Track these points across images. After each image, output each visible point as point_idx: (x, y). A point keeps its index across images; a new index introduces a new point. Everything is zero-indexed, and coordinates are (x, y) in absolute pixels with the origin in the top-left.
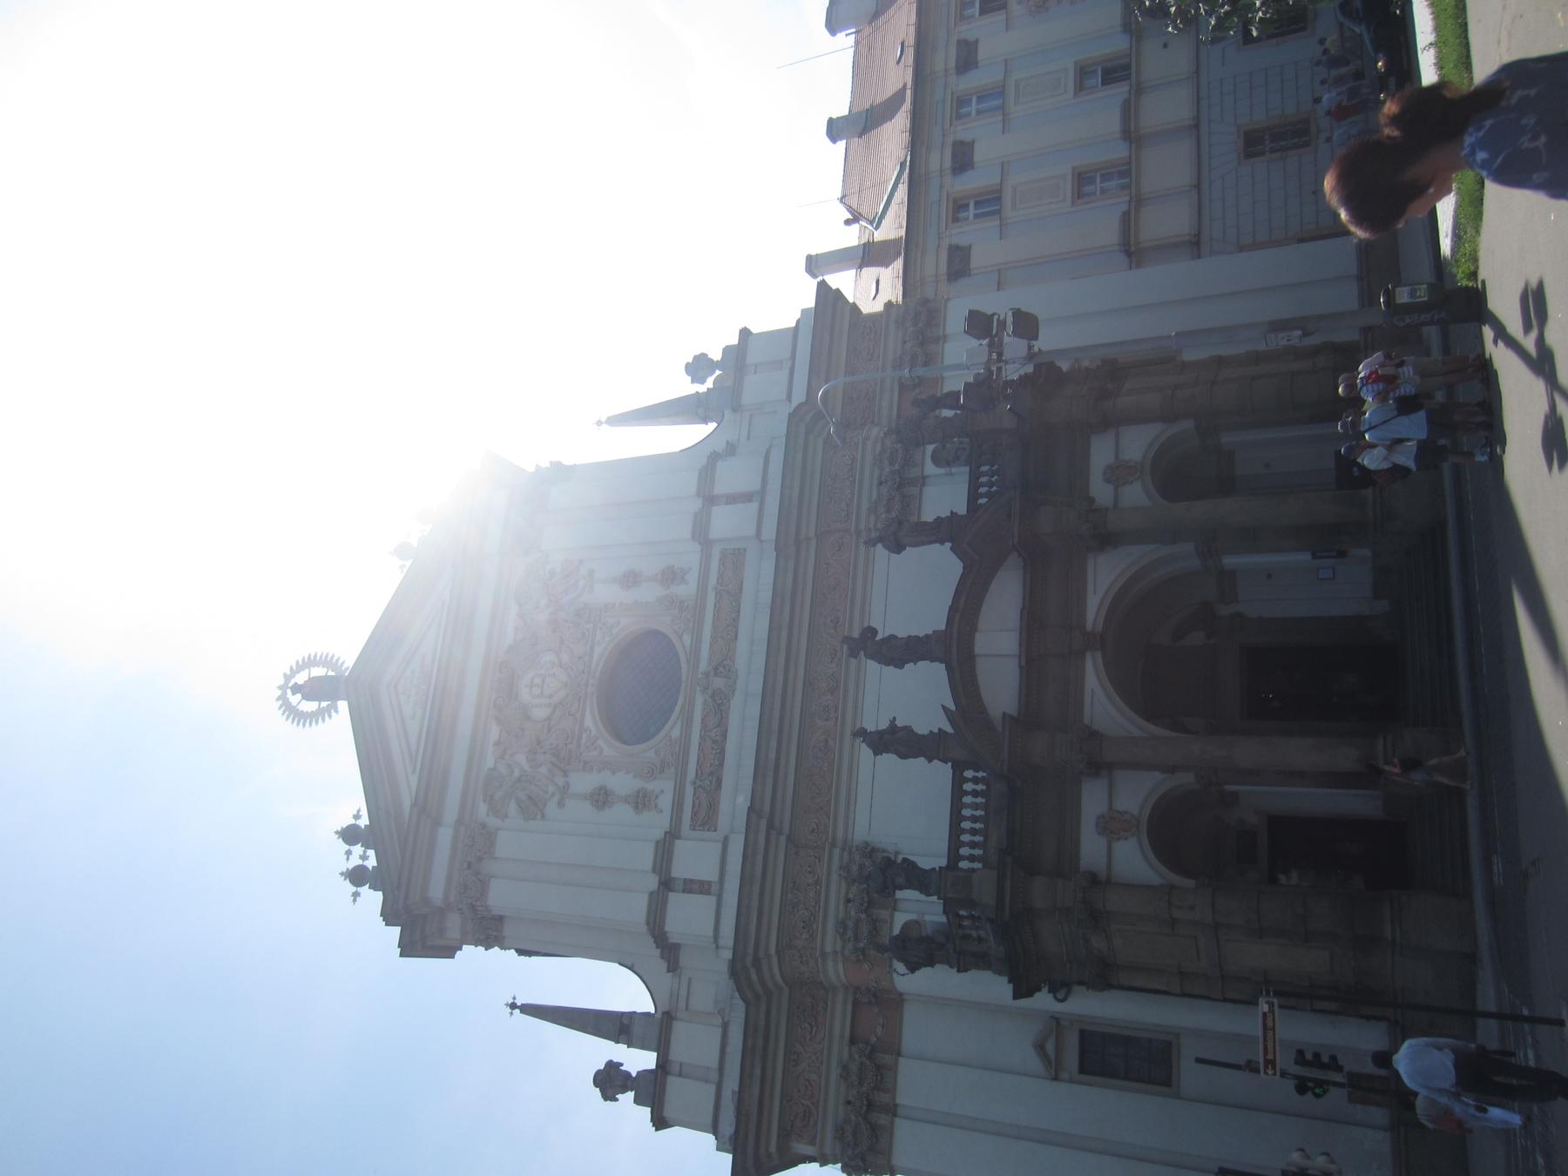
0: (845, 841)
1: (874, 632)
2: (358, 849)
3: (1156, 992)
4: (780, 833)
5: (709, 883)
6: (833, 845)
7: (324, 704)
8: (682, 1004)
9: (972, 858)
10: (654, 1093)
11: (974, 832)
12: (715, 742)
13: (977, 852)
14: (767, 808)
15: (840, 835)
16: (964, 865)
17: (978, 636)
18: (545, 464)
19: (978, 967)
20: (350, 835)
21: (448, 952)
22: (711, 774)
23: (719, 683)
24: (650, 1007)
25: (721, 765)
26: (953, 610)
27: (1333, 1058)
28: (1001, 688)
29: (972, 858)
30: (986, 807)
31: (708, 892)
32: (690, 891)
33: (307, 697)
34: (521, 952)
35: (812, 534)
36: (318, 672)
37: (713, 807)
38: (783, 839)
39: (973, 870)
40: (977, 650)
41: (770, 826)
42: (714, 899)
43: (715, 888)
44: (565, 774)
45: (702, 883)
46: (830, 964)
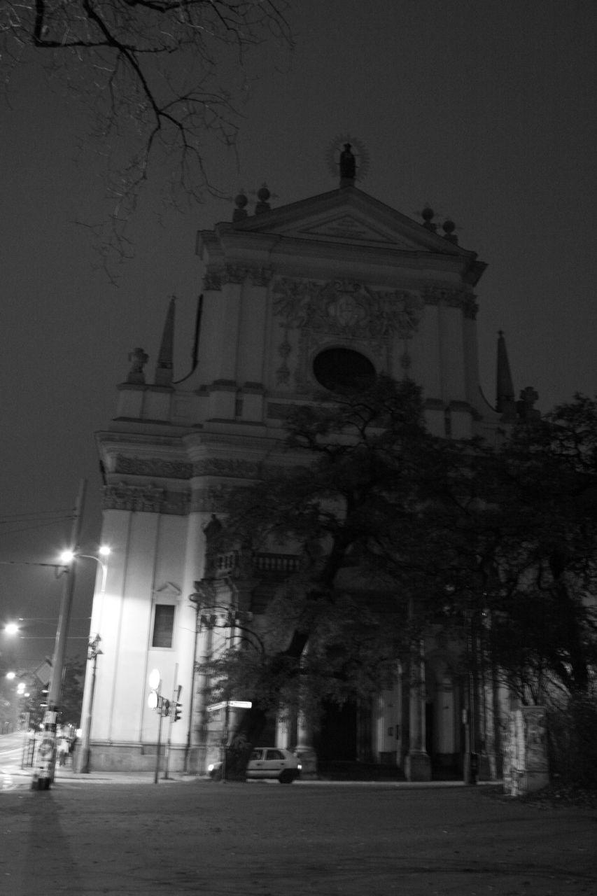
2: (256, 199)
3: (196, 643)
7: (338, 167)
10: (135, 381)
18: (477, 301)
20: (264, 194)
21: (199, 253)
24: (176, 379)
27: (179, 718)
32: (237, 404)
33: (343, 155)
34: (201, 298)
36: (358, 162)
44: (298, 327)
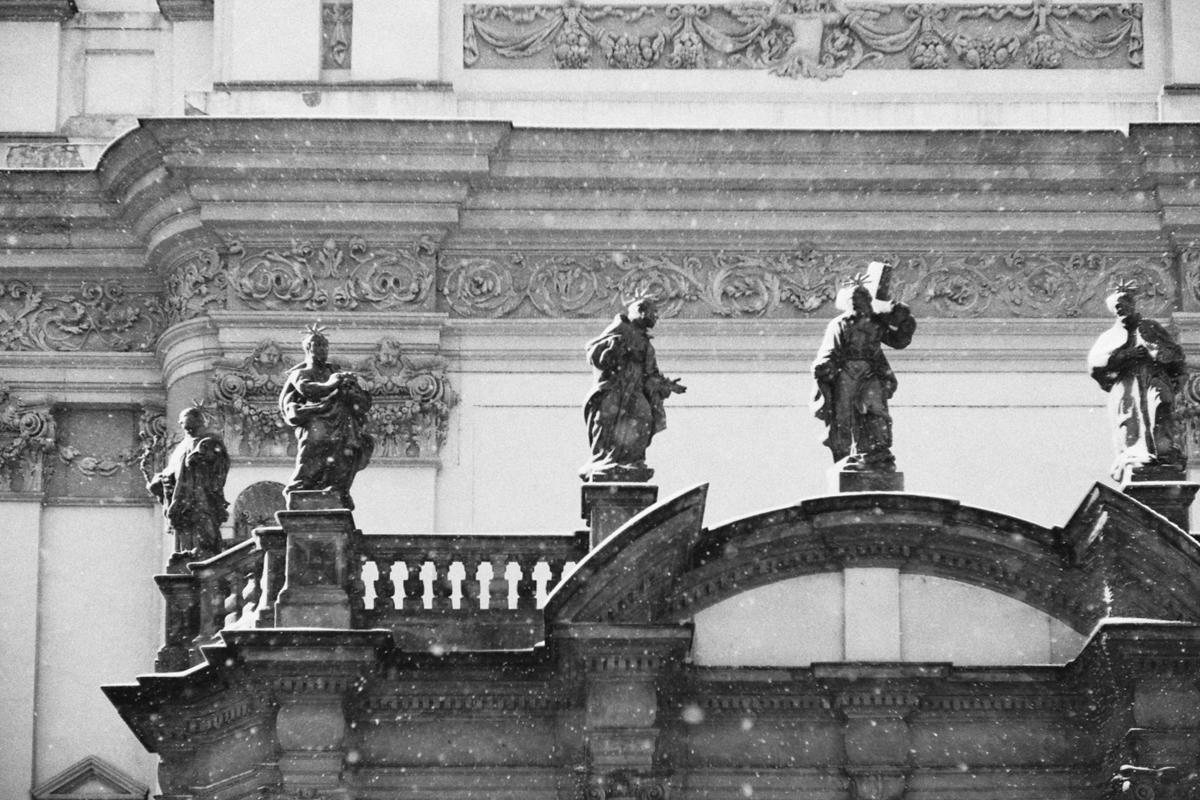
5: (346, 65)
8: (95, 41)
9: (384, 587)
11: (442, 589)
12: (669, 43)
13: (399, 599)
14: (515, 171)
16: (370, 572)
19: (172, 617)
22: (594, 43)
23: (807, 33)
25: (617, 63)
28: (751, 629)
29: (384, 587)
30: (499, 610)
31: (326, 64)
32: (327, 23)
37: (519, 52)
39: (355, 591)
42: (315, 77)
43: (335, 76)
45: (345, 46)
46: (195, 344)
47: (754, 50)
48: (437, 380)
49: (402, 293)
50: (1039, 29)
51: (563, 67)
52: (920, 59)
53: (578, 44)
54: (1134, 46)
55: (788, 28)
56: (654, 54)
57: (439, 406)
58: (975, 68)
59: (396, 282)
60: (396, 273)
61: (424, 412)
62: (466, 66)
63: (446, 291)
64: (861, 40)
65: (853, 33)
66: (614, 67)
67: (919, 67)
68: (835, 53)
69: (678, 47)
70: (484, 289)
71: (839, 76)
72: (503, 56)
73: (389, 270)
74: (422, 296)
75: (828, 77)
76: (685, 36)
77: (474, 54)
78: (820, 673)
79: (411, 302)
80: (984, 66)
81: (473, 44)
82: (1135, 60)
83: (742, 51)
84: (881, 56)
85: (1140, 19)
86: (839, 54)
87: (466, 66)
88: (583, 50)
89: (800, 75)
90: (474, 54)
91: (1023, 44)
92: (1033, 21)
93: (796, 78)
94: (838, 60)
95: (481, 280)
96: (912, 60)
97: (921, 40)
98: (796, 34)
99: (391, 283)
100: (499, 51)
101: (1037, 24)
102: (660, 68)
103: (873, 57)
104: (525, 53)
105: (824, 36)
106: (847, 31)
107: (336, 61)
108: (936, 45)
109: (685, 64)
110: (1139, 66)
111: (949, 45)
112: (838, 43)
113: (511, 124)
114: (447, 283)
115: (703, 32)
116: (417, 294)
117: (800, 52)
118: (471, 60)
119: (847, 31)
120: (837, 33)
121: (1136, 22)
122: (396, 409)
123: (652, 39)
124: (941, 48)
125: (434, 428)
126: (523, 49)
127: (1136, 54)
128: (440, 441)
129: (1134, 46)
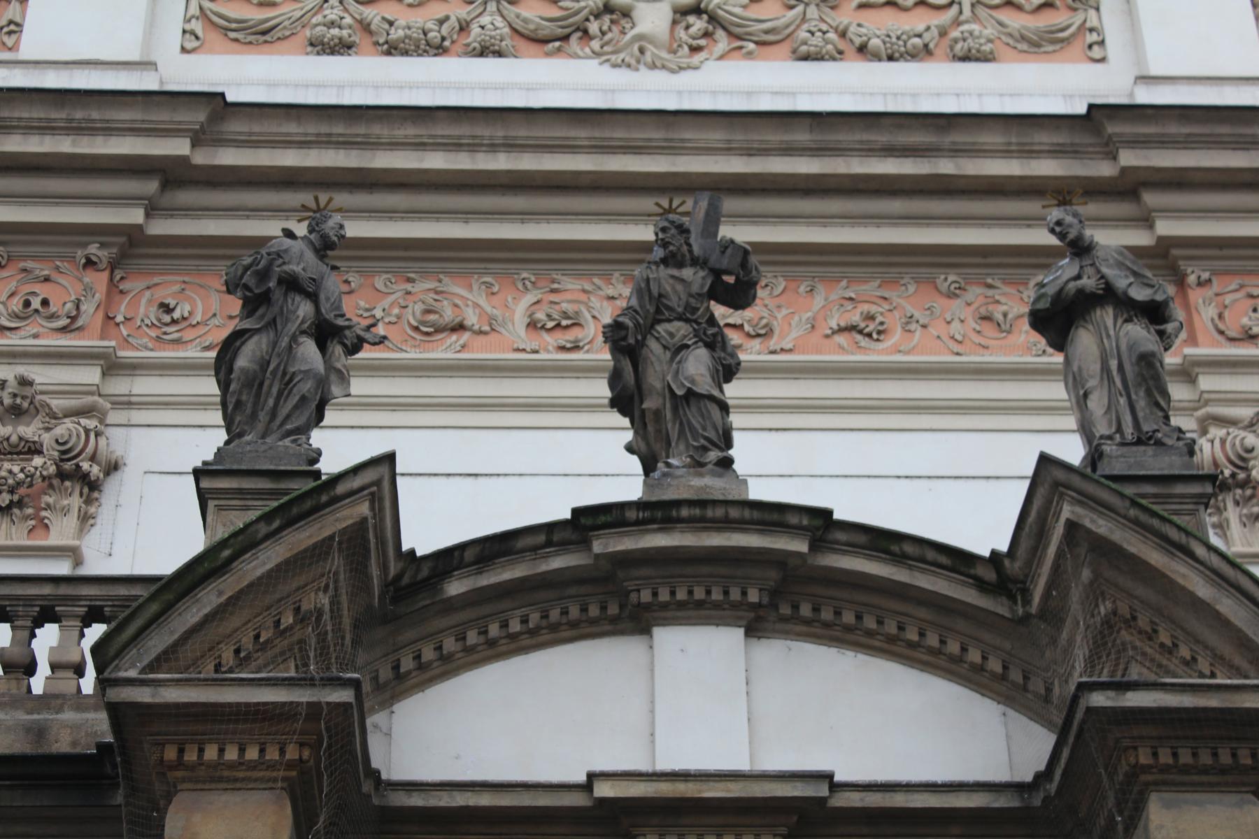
0: (127, 403)
1: (740, 296)
4: (152, 210)
6: (112, 366)
12: (464, 27)
14: (229, 157)
15: (144, 386)
17: (729, 639)
22: (365, 27)
25: (392, 49)
26: (819, 522)
35: (1165, 228)
38: (135, 216)
40: (668, 638)
41: (173, 175)
47: (581, 38)
48: (87, 431)
49: (52, 317)
50: (962, 18)
51: (318, 54)
52: (804, 48)
53: (340, 27)
54: (1094, 37)
55: (626, 14)
56: (443, 39)
57: (85, 466)
58: (880, 60)
59: (45, 303)
60: (43, 291)
61: (62, 475)
62: (184, 50)
63: (120, 318)
64: (724, 28)
65: (713, 19)
66: (388, 53)
67: (806, 58)
68: (690, 41)
69: (475, 29)
70: (176, 315)
71: (696, 68)
72: (236, 40)
73: (37, 288)
74: (80, 323)
75: (681, 68)
76: (485, 20)
77: (197, 38)
78: (604, 790)
79: (63, 330)
80: (891, 58)
81: (197, 26)
82: (1097, 52)
83: (565, 38)
84: (751, 46)
85: (1098, 9)
86: (695, 43)
87: (184, 50)
88: (345, 33)
89: (642, 67)
90: (197, 38)
91: (943, 33)
92: (955, 8)
93: (637, 70)
94: (695, 49)
95: (172, 303)
96: (794, 52)
97: (805, 27)
98: (635, 20)
99: (36, 303)
100: (233, 35)
101: (961, 12)
102: (451, 56)
103: (741, 48)
104: (267, 38)
105: (675, 22)
106: (705, 17)
107: (4, 44)
108: (824, 33)
109: (484, 51)
110: (1102, 60)
111: (843, 34)
112: (693, 30)
113: (222, 95)
114: (123, 308)
115: (511, 17)
116: (73, 319)
117: (641, 37)
118: (189, 46)
119: (705, 17)
120: (691, 19)
121: (1092, 13)
122: (16, 469)
123: (441, 22)
124: (832, 36)
125: (75, 501)
126: (264, 33)
127: (1096, 48)
128: (86, 519)
129: (1094, 37)
